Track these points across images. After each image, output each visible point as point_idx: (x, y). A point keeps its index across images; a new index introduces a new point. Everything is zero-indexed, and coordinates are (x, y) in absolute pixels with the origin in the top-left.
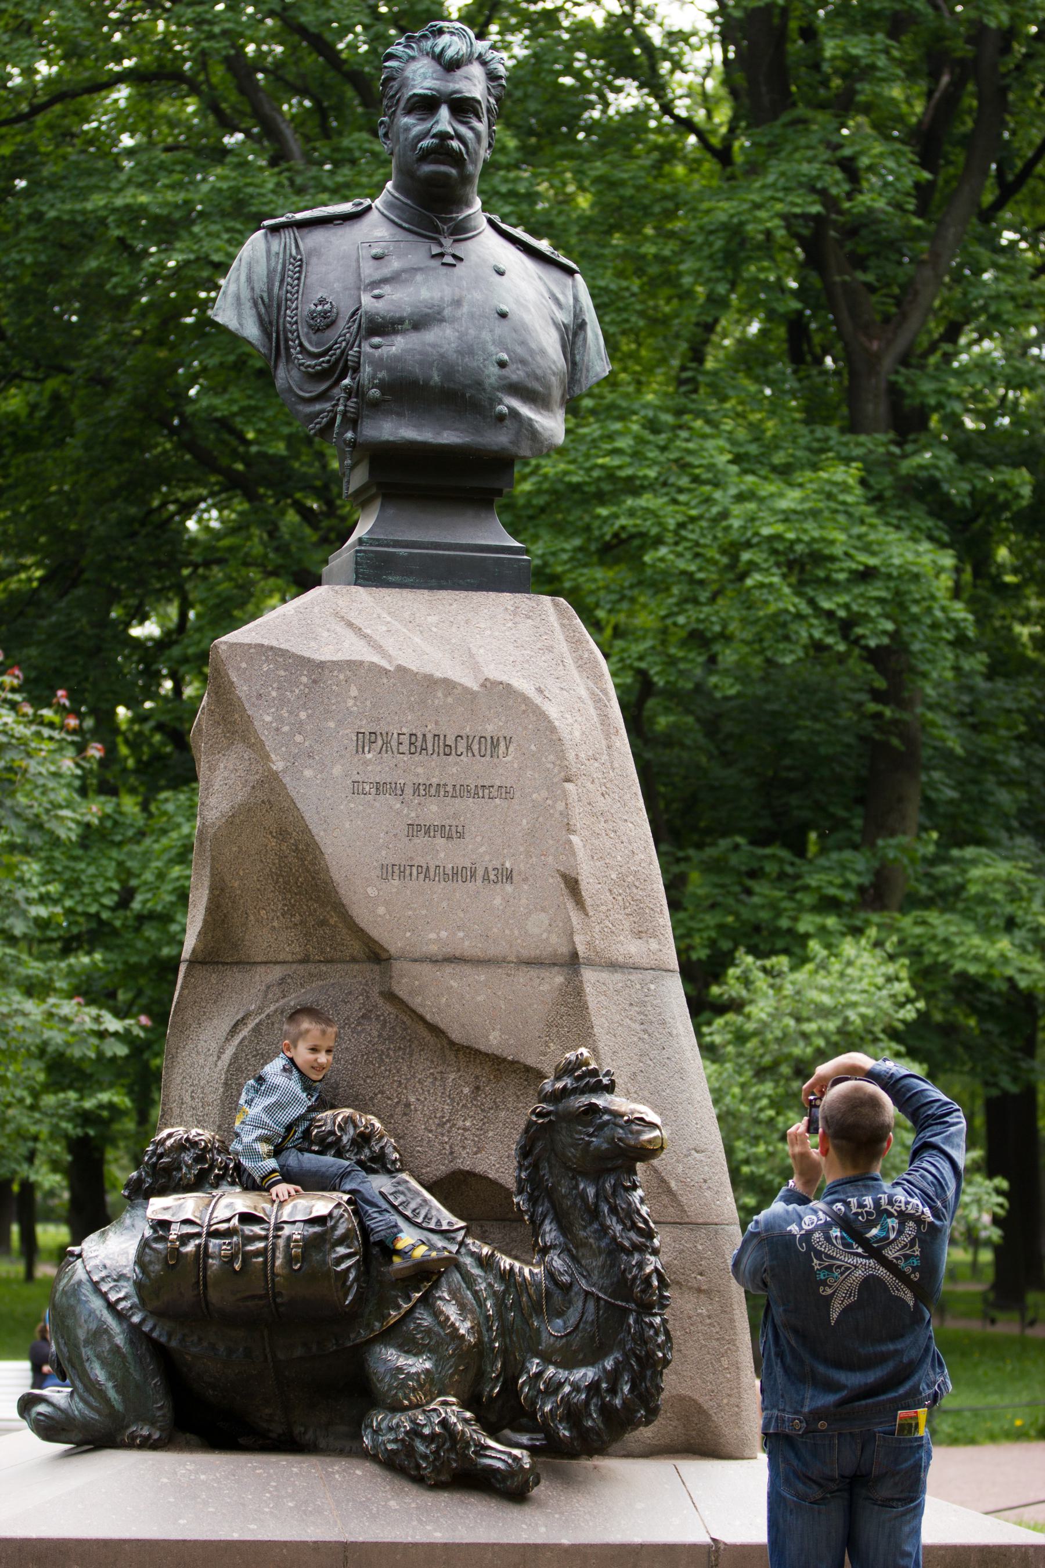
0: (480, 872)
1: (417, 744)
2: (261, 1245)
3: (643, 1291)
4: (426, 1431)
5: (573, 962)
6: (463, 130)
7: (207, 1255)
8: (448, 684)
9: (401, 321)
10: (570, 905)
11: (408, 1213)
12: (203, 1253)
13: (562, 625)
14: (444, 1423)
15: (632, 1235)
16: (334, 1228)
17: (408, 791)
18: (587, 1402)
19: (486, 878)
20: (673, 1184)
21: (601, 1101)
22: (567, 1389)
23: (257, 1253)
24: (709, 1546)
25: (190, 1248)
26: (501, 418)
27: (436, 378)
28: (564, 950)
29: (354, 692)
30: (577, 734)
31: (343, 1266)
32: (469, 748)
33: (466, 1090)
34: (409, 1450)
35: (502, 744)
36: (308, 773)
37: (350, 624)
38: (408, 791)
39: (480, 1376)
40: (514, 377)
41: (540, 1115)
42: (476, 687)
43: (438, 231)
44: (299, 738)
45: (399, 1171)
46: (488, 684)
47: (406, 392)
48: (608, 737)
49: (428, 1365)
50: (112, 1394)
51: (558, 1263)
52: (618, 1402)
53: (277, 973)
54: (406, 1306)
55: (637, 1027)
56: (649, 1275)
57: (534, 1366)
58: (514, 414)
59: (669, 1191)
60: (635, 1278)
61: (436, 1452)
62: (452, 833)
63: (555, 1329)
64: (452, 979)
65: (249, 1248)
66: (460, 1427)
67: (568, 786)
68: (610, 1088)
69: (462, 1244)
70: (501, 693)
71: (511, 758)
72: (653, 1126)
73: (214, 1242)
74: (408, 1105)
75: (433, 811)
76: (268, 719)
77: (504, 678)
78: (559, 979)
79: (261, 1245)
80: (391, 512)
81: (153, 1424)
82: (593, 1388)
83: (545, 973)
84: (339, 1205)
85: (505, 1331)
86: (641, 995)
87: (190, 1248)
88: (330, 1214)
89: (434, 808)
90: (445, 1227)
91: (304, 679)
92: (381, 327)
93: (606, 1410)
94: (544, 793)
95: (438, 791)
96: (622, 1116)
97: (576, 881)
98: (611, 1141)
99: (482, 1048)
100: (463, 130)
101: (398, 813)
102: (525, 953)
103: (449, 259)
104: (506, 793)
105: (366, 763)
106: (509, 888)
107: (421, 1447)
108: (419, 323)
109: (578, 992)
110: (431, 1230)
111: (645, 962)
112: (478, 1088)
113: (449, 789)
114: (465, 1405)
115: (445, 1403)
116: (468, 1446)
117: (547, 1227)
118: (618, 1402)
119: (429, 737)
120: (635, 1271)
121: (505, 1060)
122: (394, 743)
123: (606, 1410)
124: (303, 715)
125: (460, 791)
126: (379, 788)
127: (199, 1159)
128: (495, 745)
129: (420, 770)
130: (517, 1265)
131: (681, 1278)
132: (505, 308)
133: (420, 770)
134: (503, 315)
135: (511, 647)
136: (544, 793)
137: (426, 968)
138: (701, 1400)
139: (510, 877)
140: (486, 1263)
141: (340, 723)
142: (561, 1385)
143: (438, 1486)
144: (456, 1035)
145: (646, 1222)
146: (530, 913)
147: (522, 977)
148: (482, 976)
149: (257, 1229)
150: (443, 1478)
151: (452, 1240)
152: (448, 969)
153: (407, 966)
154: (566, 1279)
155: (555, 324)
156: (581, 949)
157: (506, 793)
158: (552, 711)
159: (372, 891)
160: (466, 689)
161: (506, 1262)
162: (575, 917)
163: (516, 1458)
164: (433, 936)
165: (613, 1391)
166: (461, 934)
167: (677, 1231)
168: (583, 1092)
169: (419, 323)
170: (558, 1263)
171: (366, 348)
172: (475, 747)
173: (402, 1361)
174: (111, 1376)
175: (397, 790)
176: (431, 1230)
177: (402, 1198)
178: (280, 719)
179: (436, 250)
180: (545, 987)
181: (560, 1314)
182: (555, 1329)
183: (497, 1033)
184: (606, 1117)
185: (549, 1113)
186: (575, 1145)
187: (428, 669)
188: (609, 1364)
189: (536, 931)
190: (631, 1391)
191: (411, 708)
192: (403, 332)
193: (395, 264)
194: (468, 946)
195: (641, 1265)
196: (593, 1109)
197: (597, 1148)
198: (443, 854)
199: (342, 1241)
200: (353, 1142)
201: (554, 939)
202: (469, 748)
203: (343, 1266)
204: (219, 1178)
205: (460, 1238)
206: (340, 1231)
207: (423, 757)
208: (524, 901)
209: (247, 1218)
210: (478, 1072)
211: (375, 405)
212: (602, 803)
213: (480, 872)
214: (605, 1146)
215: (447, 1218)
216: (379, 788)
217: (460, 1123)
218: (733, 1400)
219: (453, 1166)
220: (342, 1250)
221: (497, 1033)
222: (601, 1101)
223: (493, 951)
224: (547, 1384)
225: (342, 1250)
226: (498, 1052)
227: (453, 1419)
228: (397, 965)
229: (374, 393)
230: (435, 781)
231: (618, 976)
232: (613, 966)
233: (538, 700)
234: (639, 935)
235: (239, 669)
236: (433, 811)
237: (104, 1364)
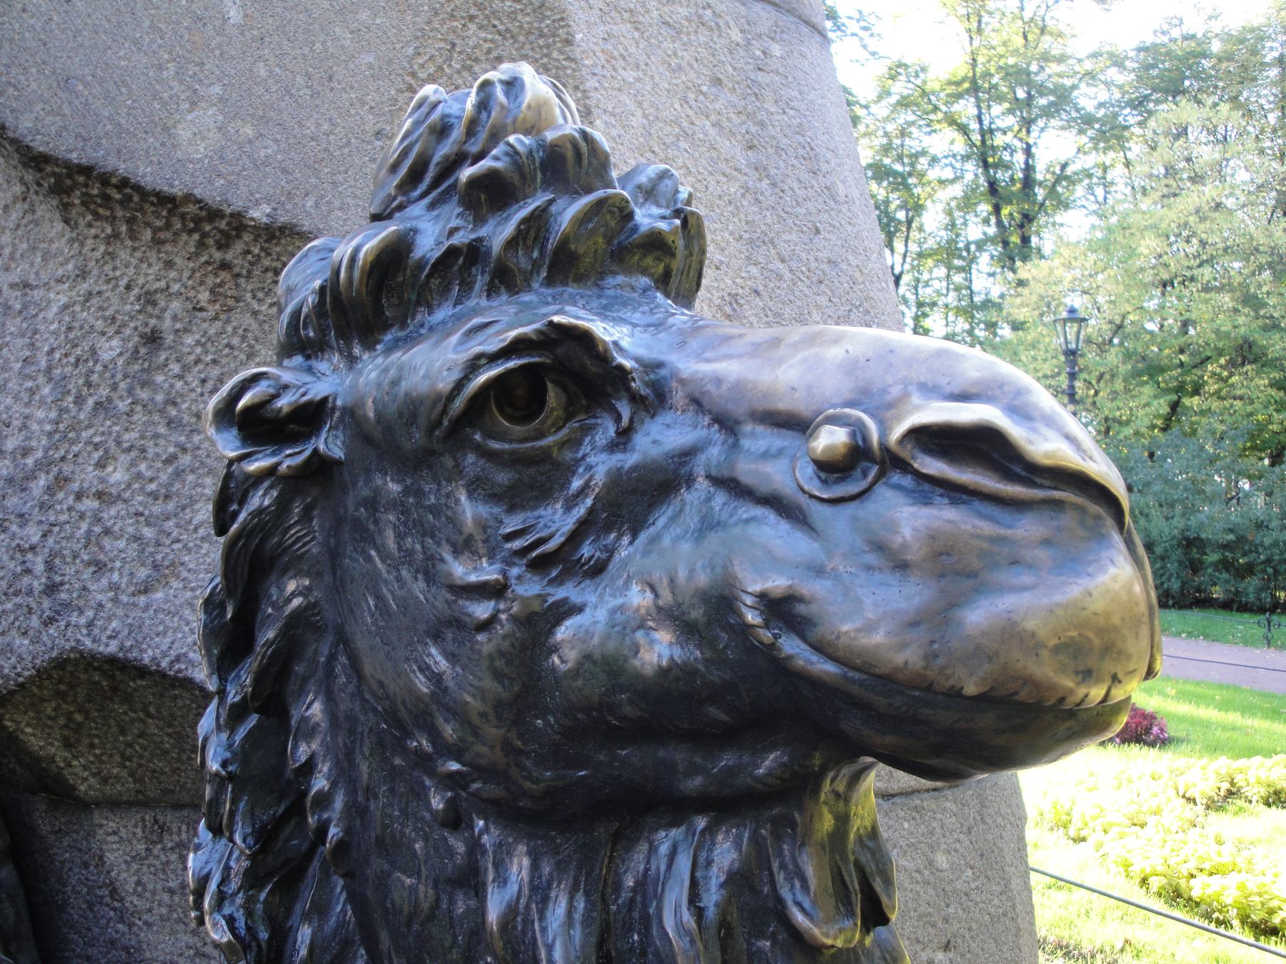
33: (110, 349)
41: (258, 425)
96: (798, 425)
98: (709, 614)
112: (153, 339)
121: (238, 224)
168: (505, 279)
183: (208, 116)
184: (662, 437)
185: (311, 416)
186: (448, 629)
197: (609, 667)
210: (151, 275)
214: (659, 649)
217: (87, 475)
219: (57, 640)
221: (208, 116)
226: (210, 191)
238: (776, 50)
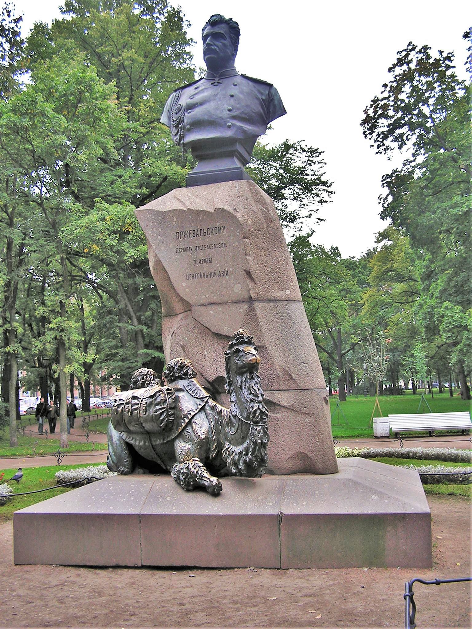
0: (218, 273)
1: (195, 233)
2: (136, 406)
3: (253, 417)
4: (182, 471)
5: (250, 300)
6: (217, 43)
7: (124, 411)
8: (204, 212)
9: (197, 104)
10: (248, 281)
11: (191, 392)
12: (123, 410)
13: (251, 189)
14: (188, 468)
15: (251, 397)
16: (156, 399)
17: (193, 249)
18: (239, 460)
19: (220, 275)
20: (293, 376)
21: (241, 348)
22: (234, 454)
23: (136, 409)
24: (278, 516)
25: (120, 409)
26: (229, 127)
27: (206, 118)
28: (247, 296)
29: (175, 220)
30: (250, 222)
31: (158, 413)
32: (212, 232)
33: (220, 348)
34: (178, 477)
35: (222, 229)
36: (162, 248)
37: (178, 199)
38: (193, 249)
39: (208, 450)
40: (235, 114)
41: (226, 354)
42: (213, 212)
43: (215, 77)
44: (159, 237)
45: (192, 378)
46: (217, 210)
47: (197, 124)
48: (267, 223)
49: (190, 446)
50: (114, 457)
51: (233, 408)
52: (248, 459)
53: (181, 316)
54: (184, 425)
55: (280, 321)
56: (255, 411)
57: (227, 444)
58: (233, 125)
59: (292, 378)
60: (251, 412)
61: (185, 479)
62: (208, 261)
63: (231, 431)
64: (211, 311)
65: (133, 408)
66: (192, 469)
67: (246, 240)
68: (249, 343)
69: (207, 402)
70: (221, 212)
71: (225, 233)
72: (252, 354)
73: (127, 406)
74: (205, 355)
75: (201, 255)
76: (150, 233)
77: (222, 207)
78: (246, 307)
79: (136, 406)
80: (201, 164)
81: (124, 466)
82: (241, 453)
83: (241, 305)
84: (160, 391)
85: (218, 433)
86: (281, 310)
87: (120, 409)
88: (155, 395)
89: (202, 254)
90: (201, 397)
91: (160, 218)
92: (190, 107)
93: (245, 461)
94: (237, 243)
95: (202, 248)
97: (250, 272)
99: (222, 334)
100: (217, 43)
101: (191, 257)
102: (234, 299)
103: (217, 84)
104: (224, 245)
105: (180, 242)
106: (227, 277)
107: (182, 477)
108: (201, 104)
109: (253, 310)
110: (197, 398)
111: (284, 298)
112: (224, 347)
113: (206, 246)
114: (201, 462)
115: (194, 460)
116: (196, 476)
117: (232, 395)
118: (248, 459)
119: (199, 230)
120: (251, 410)
122: (188, 234)
123: (245, 461)
124: (160, 230)
125: (209, 247)
126: (184, 250)
127: (143, 378)
128: (220, 230)
129: (197, 242)
130: (223, 408)
131: (298, 410)
132: (232, 94)
133: (197, 242)
134: (232, 96)
135: (227, 197)
136: (237, 243)
137: (202, 308)
138: (307, 453)
139: (227, 274)
140: (213, 408)
141: (171, 230)
142: (233, 452)
143: (188, 491)
144: (214, 330)
145: (255, 391)
146: (234, 286)
147: (233, 307)
148: (220, 308)
149: (136, 401)
150: (191, 488)
151: (203, 401)
152: (209, 307)
153: (197, 308)
154: (234, 414)
155: (257, 98)
156: (253, 296)
157: (224, 245)
158: (239, 215)
159: (184, 284)
160: (209, 212)
161: (219, 407)
162: (250, 285)
163: (211, 481)
164: (204, 297)
165: (247, 454)
166: (213, 295)
167: (296, 392)
169: (201, 104)
170: (233, 408)
171: (186, 114)
172: (213, 231)
173: (184, 444)
174: (113, 451)
175: (190, 250)
176: (197, 398)
177: (190, 387)
178: (153, 232)
179: (212, 82)
180: (241, 310)
181: (234, 427)
182: (231, 431)
187: (197, 209)
188: (245, 445)
189: (237, 291)
190: (252, 455)
191: (193, 222)
192: (198, 106)
193: (200, 89)
194: (215, 299)
195: (252, 407)
196: (238, 351)
198: (205, 268)
199: (158, 404)
200: (178, 369)
201: (243, 293)
202: (212, 232)
203: (158, 413)
204: (148, 384)
205: (206, 400)
206: (159, 400)
207: (198, 237)
208: (232, 281)
209: (134, 397)
211: (189, 130)
212: (263, 245)
213: (218, 273)
215: (204, 393)
216: (184, 250)
217: (219, 360)
218: (320, 453)
219: (217, 375)
220: (158, 407)
221: (226, 328)
222: (241, 348)
223: (225, 299)
224: (229, 452)
225: (158, 407)
227: (191, 467)
228: (193, 308)
229: (188, 127)
230: (201, 245)
231: (272, 304)
232: (269, 301)
233: (233, 212)
234: (282, 289)
235: (141, 218)
236: (201, 255)
237: (113, 447)
238: (287, 307)
